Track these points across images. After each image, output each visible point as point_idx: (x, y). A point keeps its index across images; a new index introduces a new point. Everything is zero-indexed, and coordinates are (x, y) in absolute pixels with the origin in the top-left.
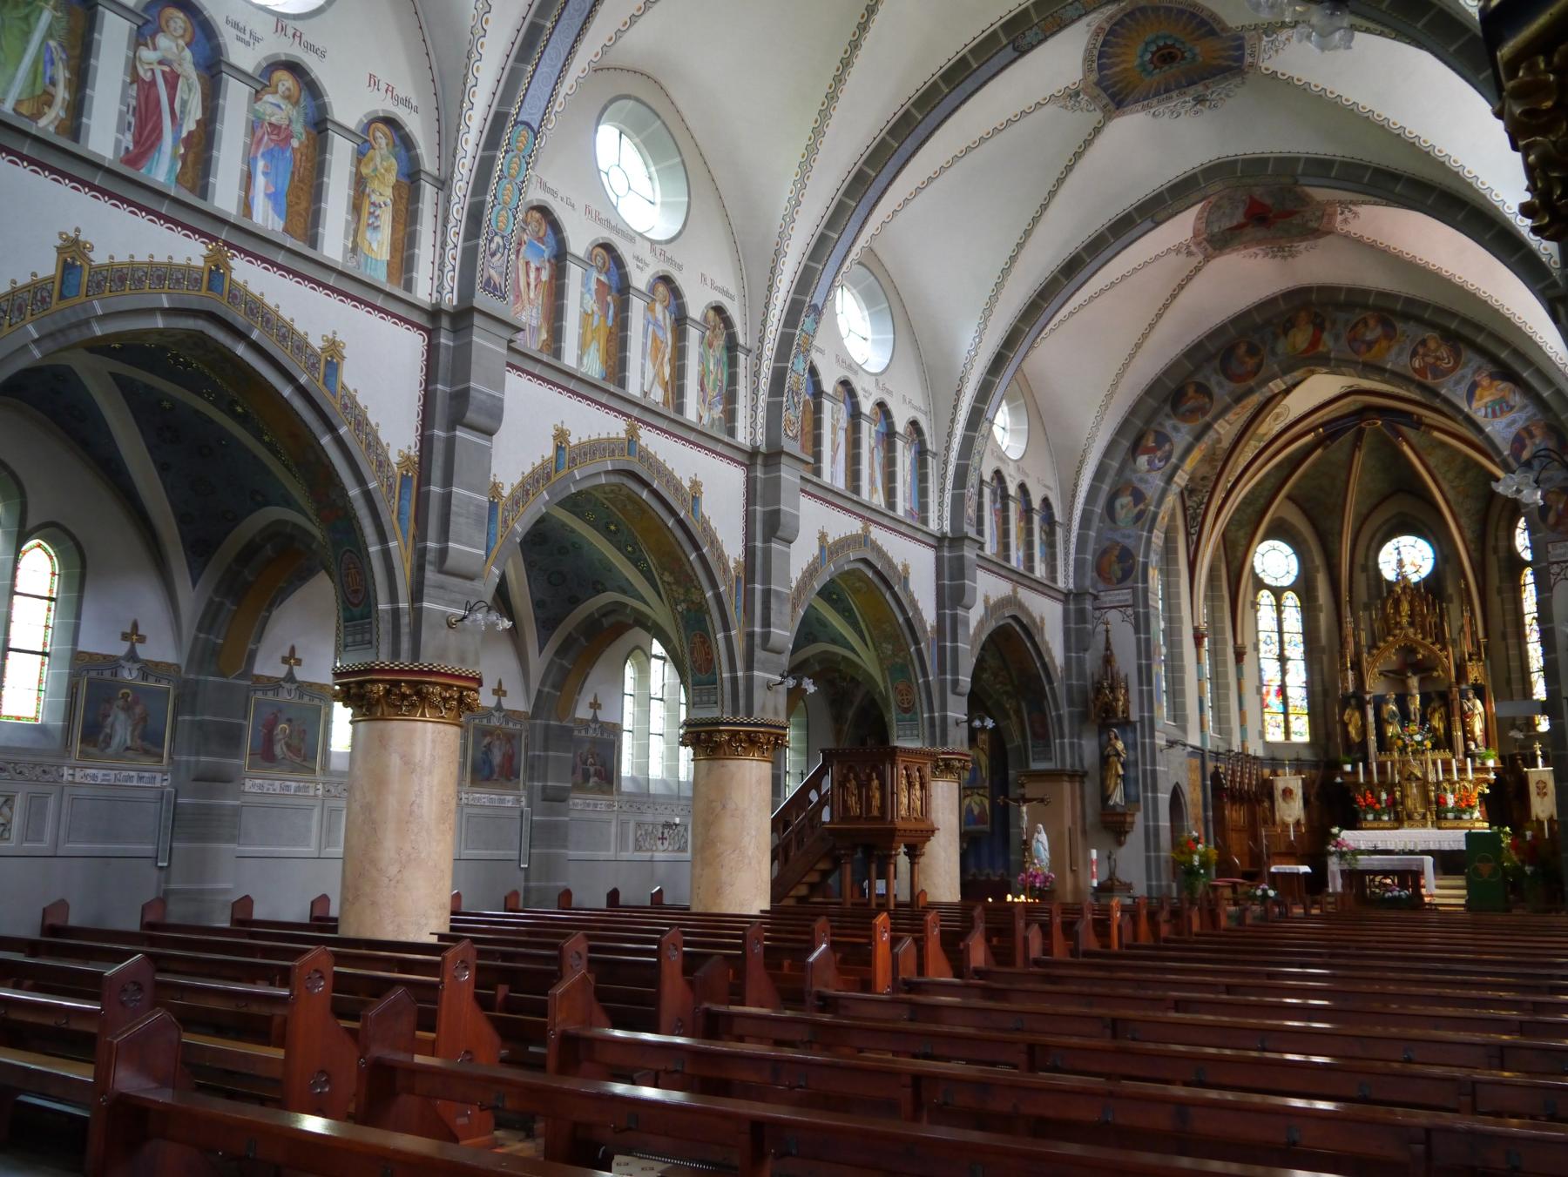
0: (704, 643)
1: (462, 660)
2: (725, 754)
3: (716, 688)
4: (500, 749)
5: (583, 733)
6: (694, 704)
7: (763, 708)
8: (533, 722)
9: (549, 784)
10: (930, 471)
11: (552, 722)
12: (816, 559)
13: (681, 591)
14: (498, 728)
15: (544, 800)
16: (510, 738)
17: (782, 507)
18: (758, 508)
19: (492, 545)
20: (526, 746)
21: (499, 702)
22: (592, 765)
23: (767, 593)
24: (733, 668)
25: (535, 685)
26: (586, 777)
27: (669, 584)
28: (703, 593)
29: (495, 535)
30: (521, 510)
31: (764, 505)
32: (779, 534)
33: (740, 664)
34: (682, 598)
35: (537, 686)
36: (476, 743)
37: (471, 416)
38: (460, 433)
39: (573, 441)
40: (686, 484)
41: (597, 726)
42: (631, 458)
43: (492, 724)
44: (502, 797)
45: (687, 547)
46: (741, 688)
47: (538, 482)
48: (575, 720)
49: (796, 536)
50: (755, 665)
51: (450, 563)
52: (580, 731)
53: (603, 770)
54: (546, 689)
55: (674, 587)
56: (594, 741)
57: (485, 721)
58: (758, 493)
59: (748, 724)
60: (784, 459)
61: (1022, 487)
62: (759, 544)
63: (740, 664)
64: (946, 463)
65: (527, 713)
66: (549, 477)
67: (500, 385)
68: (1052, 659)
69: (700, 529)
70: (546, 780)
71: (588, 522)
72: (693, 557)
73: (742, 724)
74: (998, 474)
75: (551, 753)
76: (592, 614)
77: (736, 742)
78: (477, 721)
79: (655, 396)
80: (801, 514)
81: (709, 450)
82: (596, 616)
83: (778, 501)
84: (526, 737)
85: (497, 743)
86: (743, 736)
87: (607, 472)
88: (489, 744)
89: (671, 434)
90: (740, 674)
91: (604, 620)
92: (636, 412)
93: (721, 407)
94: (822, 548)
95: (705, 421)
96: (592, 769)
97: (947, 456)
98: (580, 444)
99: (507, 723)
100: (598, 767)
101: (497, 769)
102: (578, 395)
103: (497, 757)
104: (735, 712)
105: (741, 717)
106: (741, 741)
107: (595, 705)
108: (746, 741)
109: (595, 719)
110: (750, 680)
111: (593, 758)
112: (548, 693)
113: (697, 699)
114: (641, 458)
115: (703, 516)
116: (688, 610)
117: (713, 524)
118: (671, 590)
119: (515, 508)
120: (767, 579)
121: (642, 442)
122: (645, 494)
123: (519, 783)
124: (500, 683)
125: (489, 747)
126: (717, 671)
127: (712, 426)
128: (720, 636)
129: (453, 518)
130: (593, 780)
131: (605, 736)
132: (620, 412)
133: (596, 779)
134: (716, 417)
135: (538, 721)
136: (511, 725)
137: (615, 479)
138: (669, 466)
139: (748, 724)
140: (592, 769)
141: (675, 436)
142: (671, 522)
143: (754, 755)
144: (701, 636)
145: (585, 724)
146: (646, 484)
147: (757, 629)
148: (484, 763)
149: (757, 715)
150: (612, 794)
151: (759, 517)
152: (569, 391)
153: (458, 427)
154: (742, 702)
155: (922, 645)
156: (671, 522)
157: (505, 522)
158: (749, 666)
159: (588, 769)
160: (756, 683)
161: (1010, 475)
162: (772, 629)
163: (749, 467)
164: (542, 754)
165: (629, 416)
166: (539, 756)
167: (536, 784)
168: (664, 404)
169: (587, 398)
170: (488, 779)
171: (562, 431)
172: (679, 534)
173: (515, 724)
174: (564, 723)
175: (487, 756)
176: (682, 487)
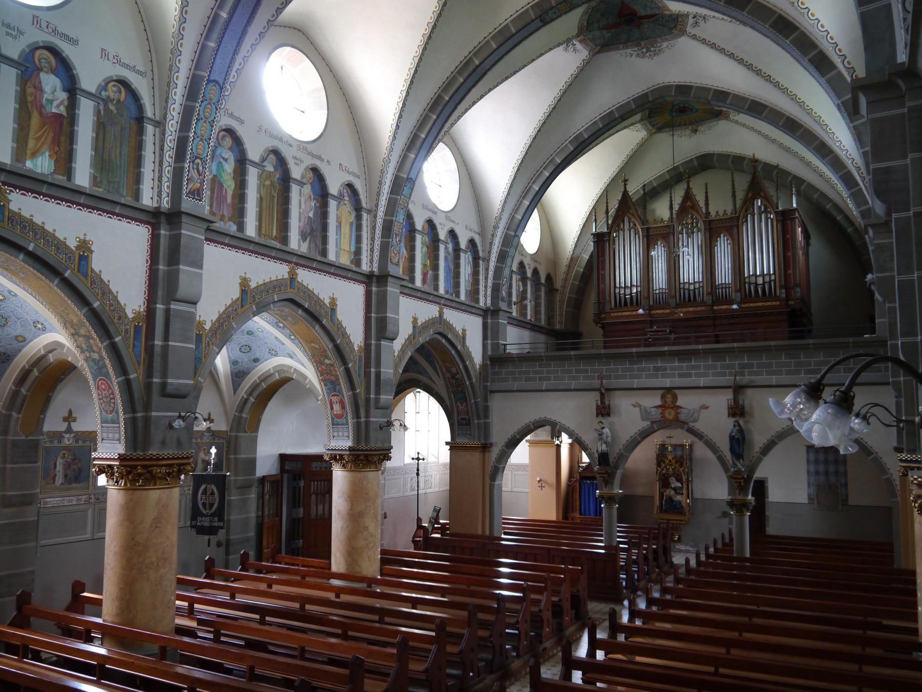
10: (364, 223)
59: (144, 459)
61: (452, 234)
64: (375, 217)
68: (472, 360)
74: (430, 223)
97: (376, 210)
131: (81, 443)
155: (350, 365)
161: (441, 224)
163: (155, 228)
176: (67, 247)
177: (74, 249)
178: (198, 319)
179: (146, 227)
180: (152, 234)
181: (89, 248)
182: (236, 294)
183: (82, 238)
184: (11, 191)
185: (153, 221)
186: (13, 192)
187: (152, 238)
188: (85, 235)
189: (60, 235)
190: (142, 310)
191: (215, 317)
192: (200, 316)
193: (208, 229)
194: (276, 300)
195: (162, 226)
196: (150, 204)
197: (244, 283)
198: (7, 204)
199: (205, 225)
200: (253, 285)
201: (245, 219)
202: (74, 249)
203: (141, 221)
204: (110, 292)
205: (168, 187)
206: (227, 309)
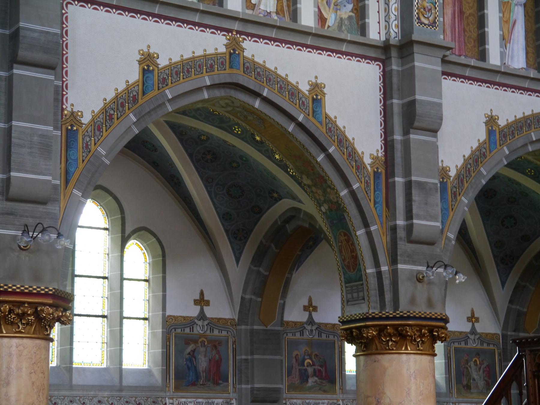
0: (348, 241)
1: (37, 278)
2: (377, 349)
3: (362, 284)
4: (205, 356)
5: (298, 335)
6: (348, 301)
7: (413, 301)
8: (238, 327)
9: (256, 386)
11: (255, 327)
12: (481, 146)
13: (320, 192)
14: (201, 336)
15: (253, 401)
16: (216, 344)
17: (418, 97)
18: (395, 101)
19: (72, 169)
20: (234, 350)
21: (202, 312)
22: (309, 365)
23: (408, 185)
24: (377, 264)
25: (238, 294)
26: (304, 377)
27: (309, 186)
28: (337, 193)
29: (77, 160)
30: (105, 134)
31: (401, 98)
32: (416, 124)
33: (383, 258)
34: (322, 198)
35: (240, 294)
36: (179, 352)
37: (22, 54)
38: (17, 71)
39: (163, 62)
40: (305, 88)
41: (314, 328)
42: (235, 71)
43: (195, 332)
44: (210, 401)
45: (313, 149)
46: (387, 283)
47: (123, 105)
48: (282, 323)
49: (440, 124)
50: (399, 258)
51: (14, 191)
52: (294, 334)
53: (323, 370)
54: (247, 297)
55: (314, 189)
56: (310, 343)
57: (187, 330)
58: (395, 87)
59: (395, 318)
60: (416, 48)
62: (398, 137)
63: (383, 258)
65: (234, 320)
66: (135, 100)
67: (62, 20)
69: (324, 130)
70: (253, 383)
71: (237, 135)
72: (321, 158)
73: (387, 318)
75: (256, 357)
76: (276, 221)
77: (385, 336)
78: (179, 331)
79: (266, 6)
80: (445, 102)
81: (332, 51)
82: (279, 223)
83: (413, 92)
84: (234, 343)
85: (202, 349)
86: (390, 330)
87: (208, 87)
88: (194, 351)
89: (282, 41)
90: (384, 268)
91: (287, 226)
92: (236, 26)
93: (350, 6)
94: (490, 133)
95: (331, 19)
96: (310, 370)
98: (170, 65)
99: (212, 330)
100: (317, 367)
101: (203, 375)
102: (166, 18)
103: (203, 363)
104: (383, 306)
105: (389, 310)
106: (390, 335)
107: (311, 308)
108: (395, 335)
109: (311, 321)
110: (395, 273)
111: (311, 359)
112: (251, 299)
113: (349, 296)
114: (246, 70)
115: (327, 116)
116: (330, 210)
117: (340, 123)
118: (312, 192)
119: (97, 133)
120: (407, 172)
121: (247, 54)
122: (257, 104)
123: (227, 386)
124: (202, 294)
125: (193, 354)
126: (362, 268)
127: (340, 27)
128: (361, 232)
129: (13, 150)
130: (311, 381)
132: (217, 28)
133: (316, 378)
134: (345, 16)
135: (243, 327)
136: (216, 332)
137: (218, 93)
138: (281, 72)
139: (395, 318)
140: (310, 370)
141: (287, 42)
142: (291, 128)
143: (406, 349)
144: (345, 235)
145: (299, 327)
146: (256, 95)
147: (401, 222)
148: (189, 368)
149: (404, 307)
150: (334, 392)
151: (396, 110)
152: (154, 15)
153: (15, 65)
154: (388, 296)
156: (291, 128)
157: (87, 146)
158: (394, 261)
159: (306, 370)
160: (401, 277)
162: (415, 221)
163: (385, 62)
164: (249, 357)
165: (229, 31)
166: (246, 360)
167: (244, 386)
168: (277, 13)
169: (177, 20)
170: (194, 384)
171: (149, 55)
172: (302, 137)
173: (220, 331)
174: (269, 327)
175: (191, 361)
176: (299, 91)
177: (307, 93)
178: (440, 164)
179: (377, 65)
180: (384, 71)
181: (322, 91)
182: (482, 136)
183: (314, 81)
184: (244, 39)
185: (383, 57)
186: (246, 40)
187: (384, 76)
188: (316, 77)
189: (292, 79)
190: (380, 155)
191: (460, 162)
192: (442, 161)
193: (444, 61)
194: (534, 139)
195: (394, 61)
196: (378, 38)
197: (491, 121)
198: (241, 53)
199: (440, 53)
200: (502, 123)
201: (487, 46)
202: (307, 93)
203: (372, 59)
204: (347, 140)
205: (397, 26)
206: (473, 153)
